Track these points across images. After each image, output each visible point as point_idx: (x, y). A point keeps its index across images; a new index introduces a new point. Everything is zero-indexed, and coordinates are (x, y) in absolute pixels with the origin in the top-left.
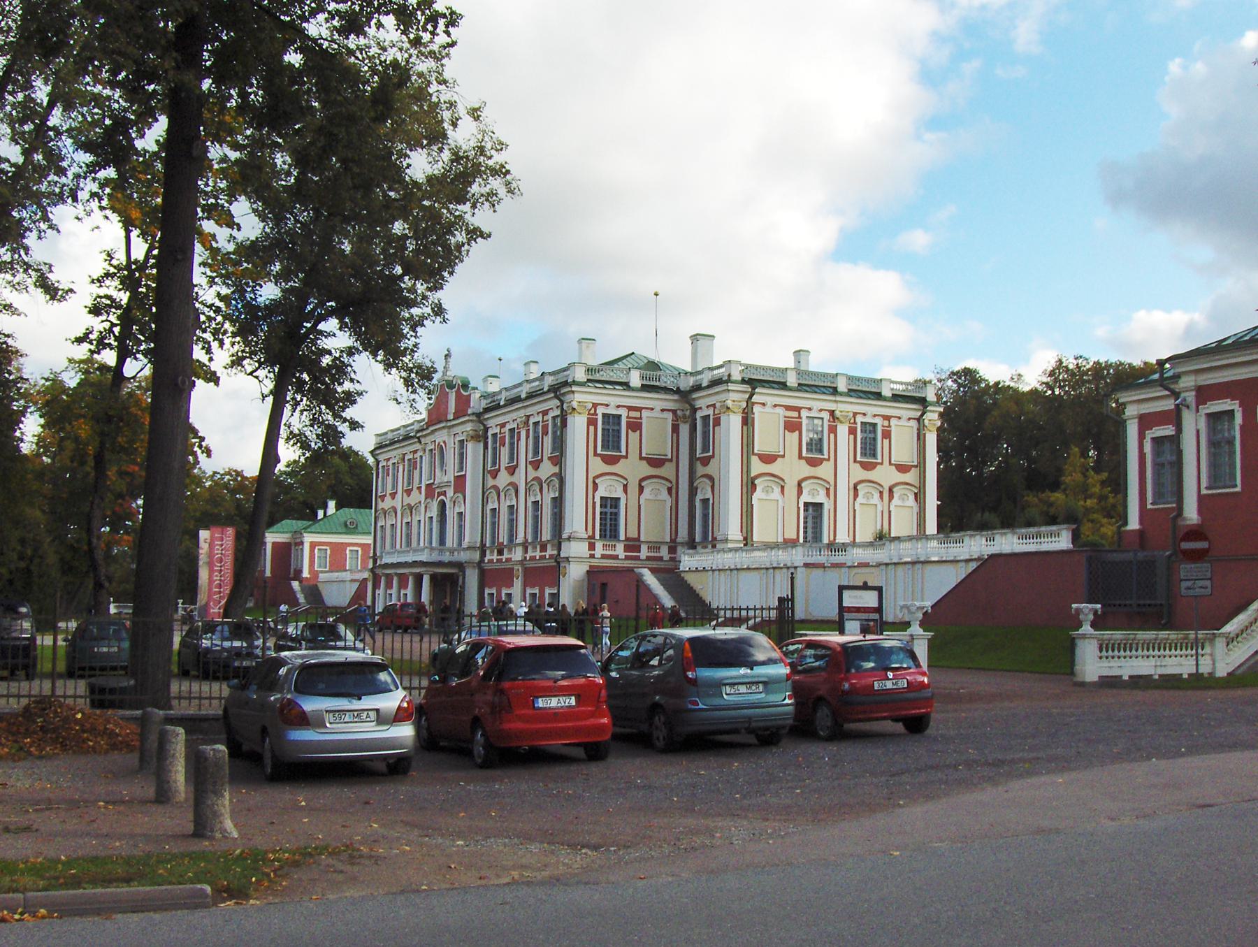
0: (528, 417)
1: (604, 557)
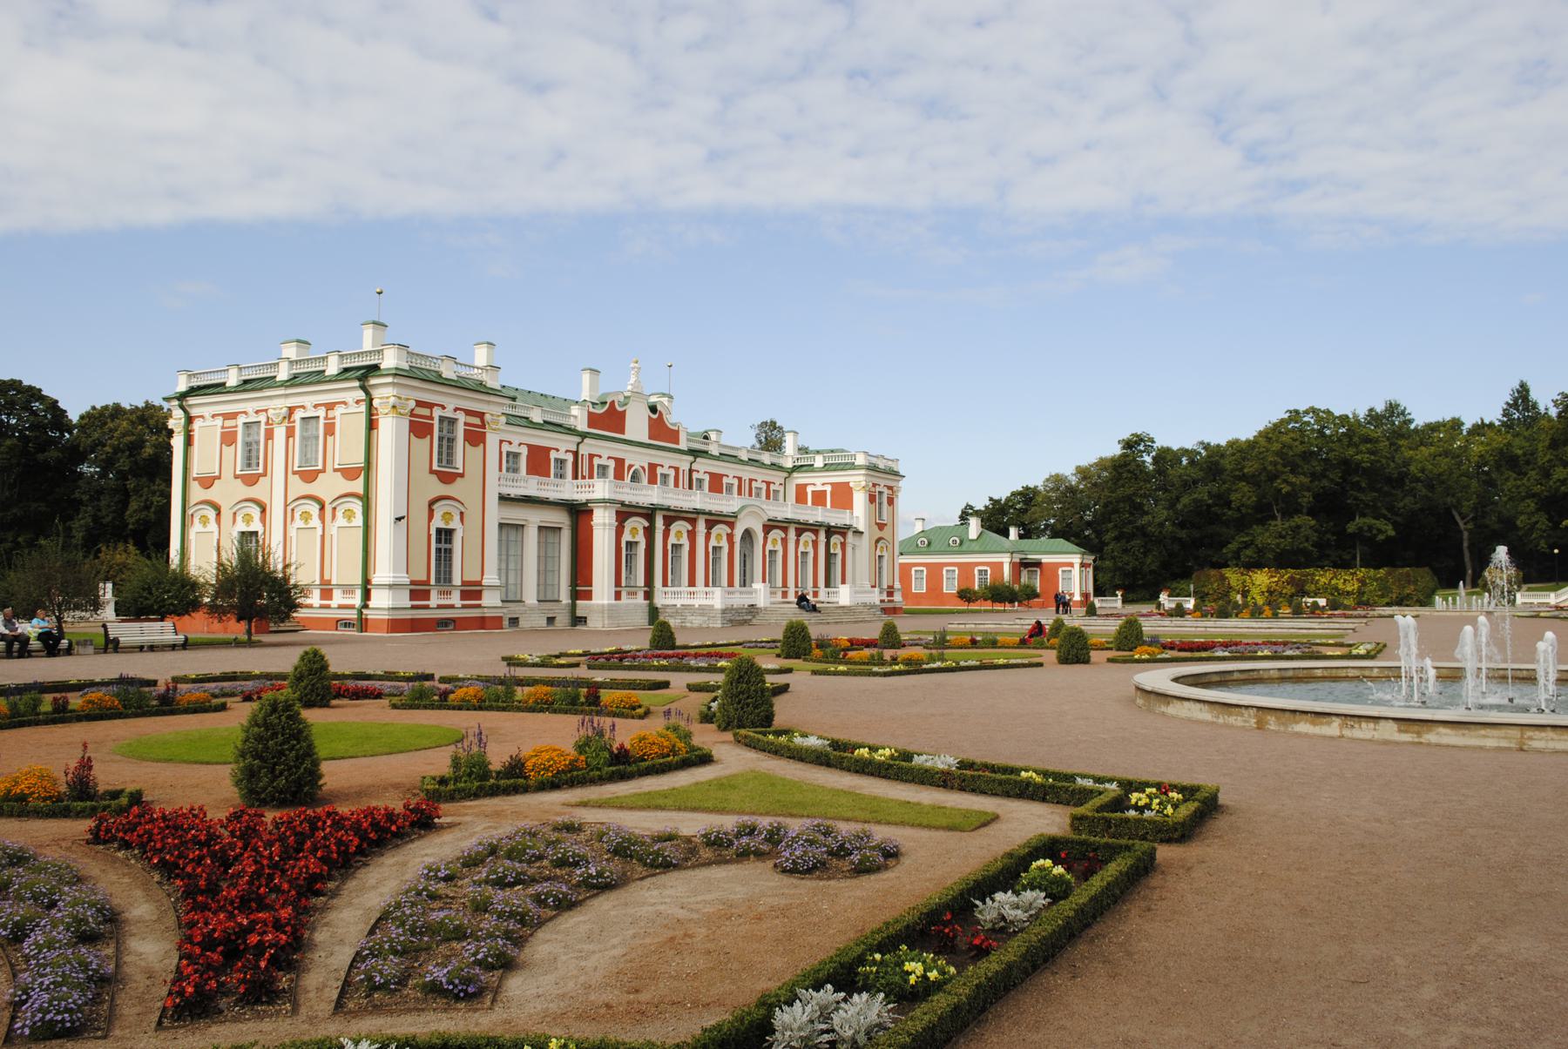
0: (291, 410)
1: (440, 607)
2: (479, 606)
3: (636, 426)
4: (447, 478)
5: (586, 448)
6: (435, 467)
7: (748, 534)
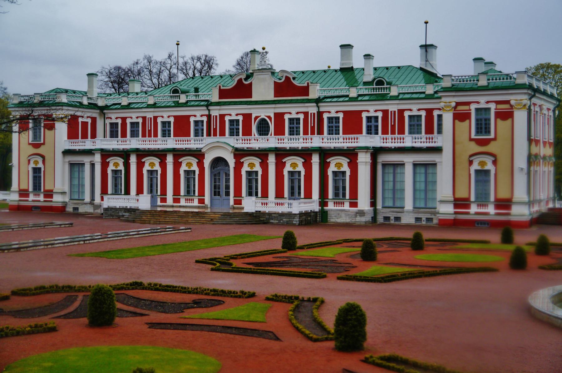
2: (51, 201)
3: (263, 89)
4: (37, 146)
5: (215, 112)
6: (30, 142)
7: (219, 162)
